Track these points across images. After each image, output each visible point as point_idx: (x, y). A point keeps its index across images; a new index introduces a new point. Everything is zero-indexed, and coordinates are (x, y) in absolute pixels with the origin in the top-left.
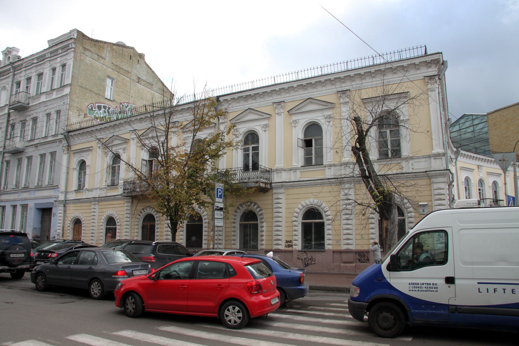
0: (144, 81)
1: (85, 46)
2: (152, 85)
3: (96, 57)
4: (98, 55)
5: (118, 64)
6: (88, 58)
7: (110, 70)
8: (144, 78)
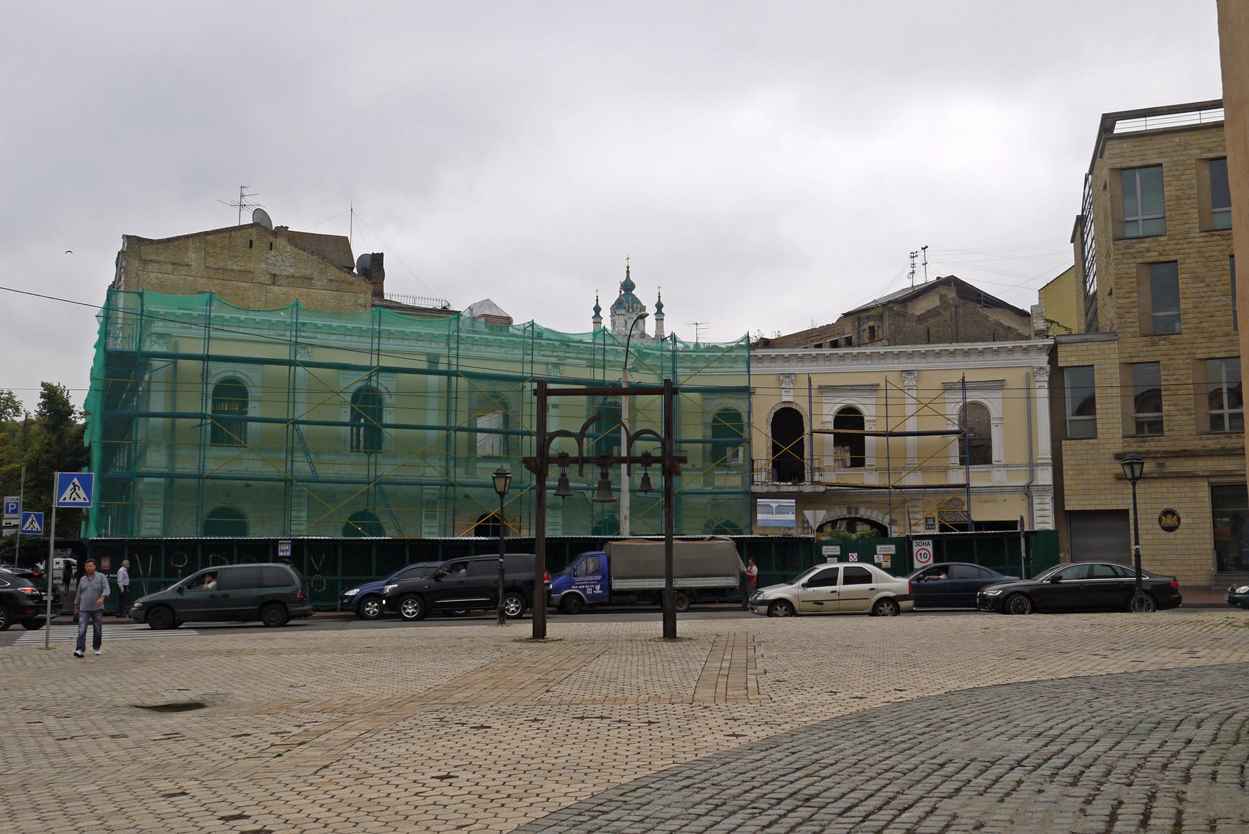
0: (287, 277)
1: (145, 257)
3: (170, 267)
4: (173, 264)
5: (221, 264)
6: (152, 275)
7: (202, 280)
8: (291, 271)
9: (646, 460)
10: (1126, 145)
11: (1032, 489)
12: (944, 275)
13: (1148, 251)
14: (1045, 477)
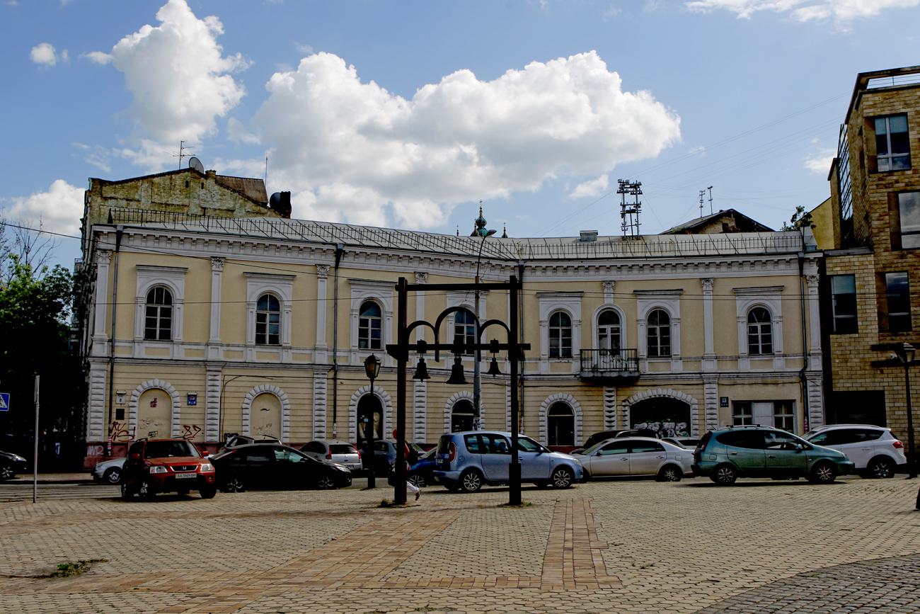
2: (233, 211)
4: (127, 200)
5: (164, 201)
9: (494, 346)
10: (878, 98)
11: (807, 374)
12: (725, 209)
13: (897, 182)
14: (816, 364)
